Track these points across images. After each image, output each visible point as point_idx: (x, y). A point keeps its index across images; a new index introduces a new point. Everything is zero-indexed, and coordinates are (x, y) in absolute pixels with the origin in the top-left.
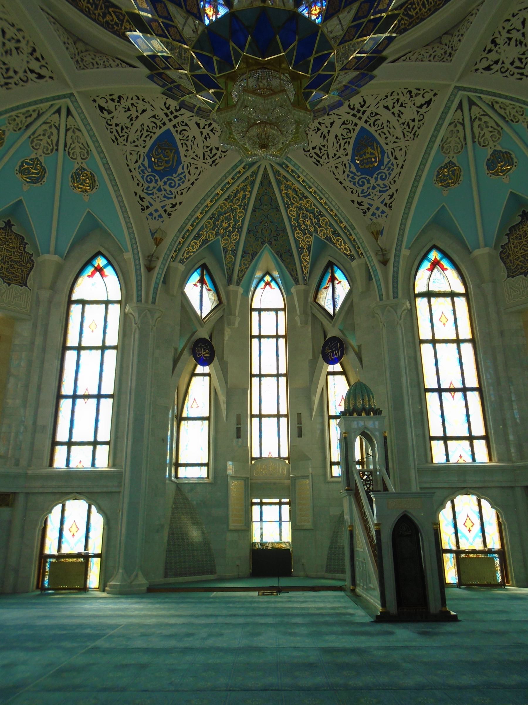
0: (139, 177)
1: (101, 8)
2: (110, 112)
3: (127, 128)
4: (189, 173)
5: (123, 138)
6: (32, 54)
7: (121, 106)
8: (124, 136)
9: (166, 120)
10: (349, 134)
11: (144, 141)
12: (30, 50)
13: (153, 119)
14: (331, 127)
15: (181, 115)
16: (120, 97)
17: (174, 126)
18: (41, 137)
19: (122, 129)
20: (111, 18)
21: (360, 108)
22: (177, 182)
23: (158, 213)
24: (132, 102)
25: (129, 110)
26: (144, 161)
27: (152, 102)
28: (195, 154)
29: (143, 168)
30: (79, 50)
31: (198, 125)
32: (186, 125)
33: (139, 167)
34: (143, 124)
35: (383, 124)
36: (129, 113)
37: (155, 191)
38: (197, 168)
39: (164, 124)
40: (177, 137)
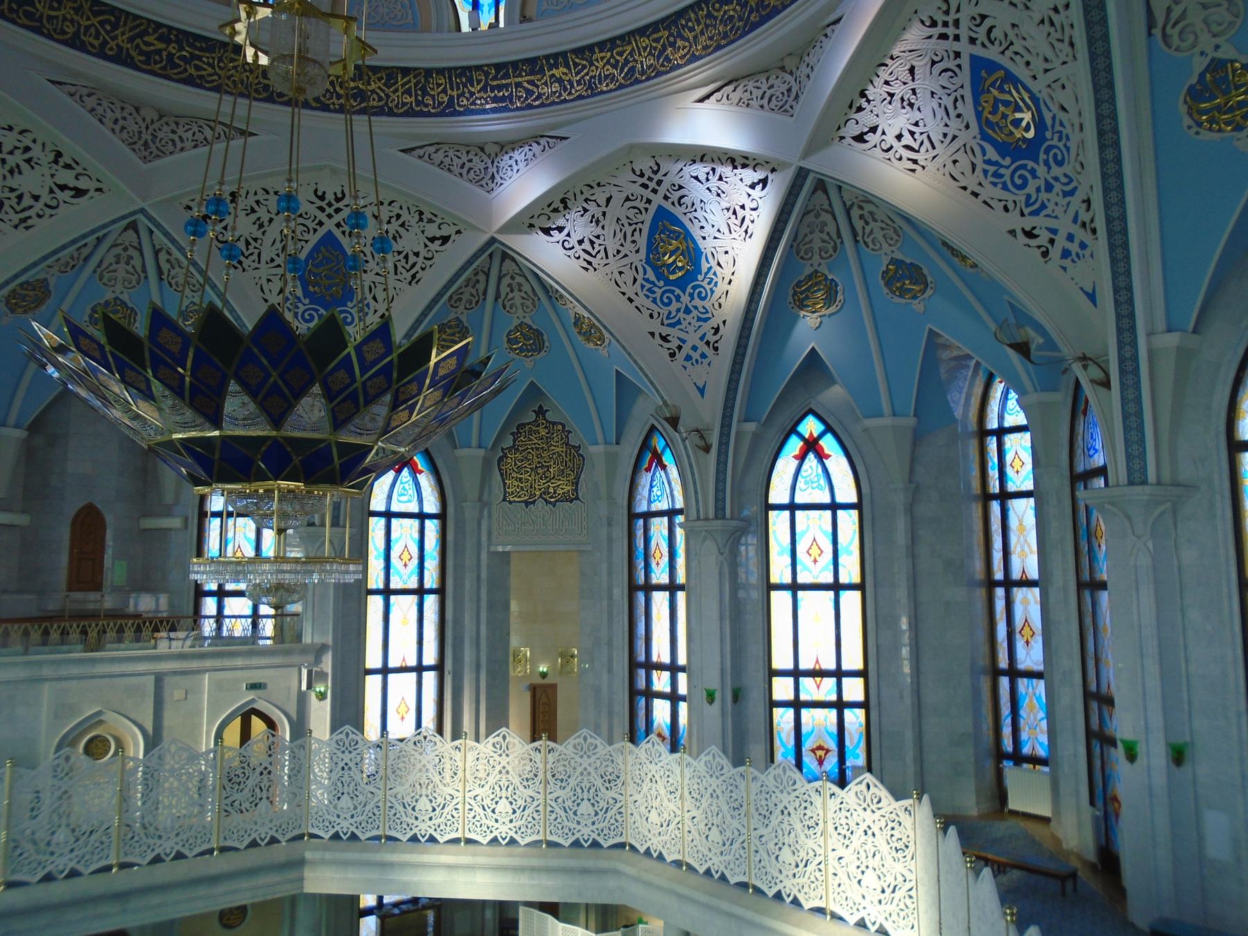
0: (648, 303)
4: (719, 264)
6: (421, 220)
9: (647, 194)
10: (954, 80)
12: (417, 218)
14: (913, 80)
18: (510, 296)
21: (946, 19)
22: (708, 287)
23: (699, 352)
24: (584, 197)
26: (645, 273)
28: (716, 229)
29: (648, 286)
33: (643, 286)
35: (1006, 35)
37: (681, 315)
38: (726, 252)
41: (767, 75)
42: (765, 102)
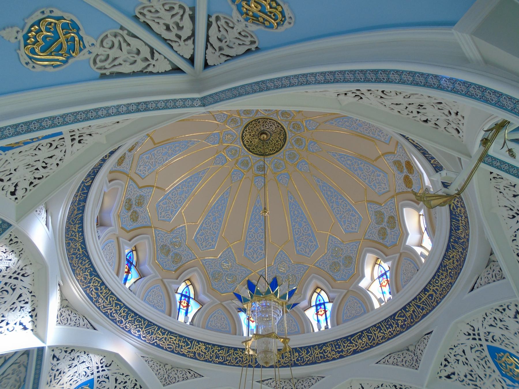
1: (394, 323)
2: (454, 374)
3: (472, 371)
5: (478, 380)
7: (453, 363)
8: (476, 378)
11: (489, 367)
13: (473, 350)
15: (478, 330)
16: (446, 360)
17: (487, 340)
19: (471, 375)
20: (400, 321)
25: (458, 360)
27: (460, 342)
30: (413, 351)
31: (491, 325)
32: (489, 333)
34: (474, 359)
36: (460, 362)
39: (481, 345)
40: (496, 345)
41: (489, 267)
42: (494, 278)
